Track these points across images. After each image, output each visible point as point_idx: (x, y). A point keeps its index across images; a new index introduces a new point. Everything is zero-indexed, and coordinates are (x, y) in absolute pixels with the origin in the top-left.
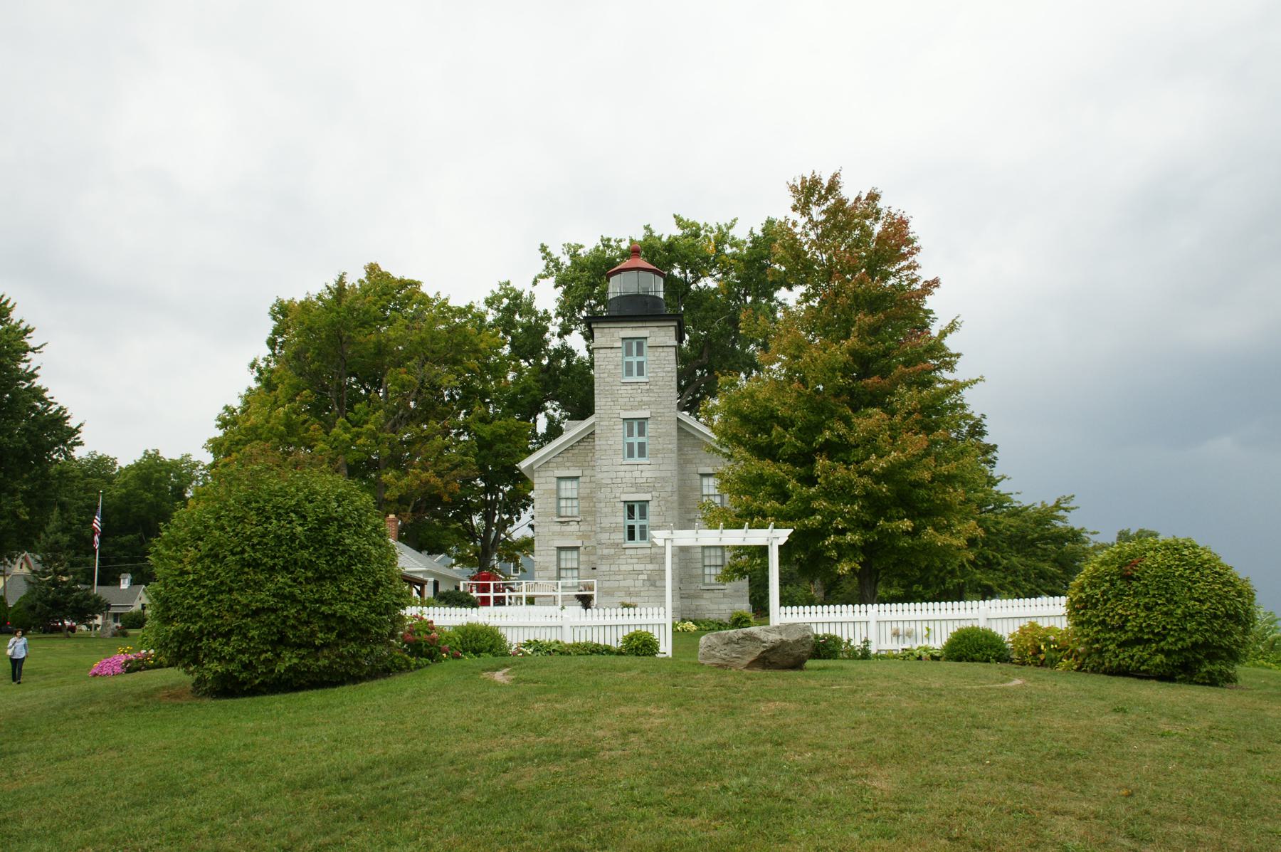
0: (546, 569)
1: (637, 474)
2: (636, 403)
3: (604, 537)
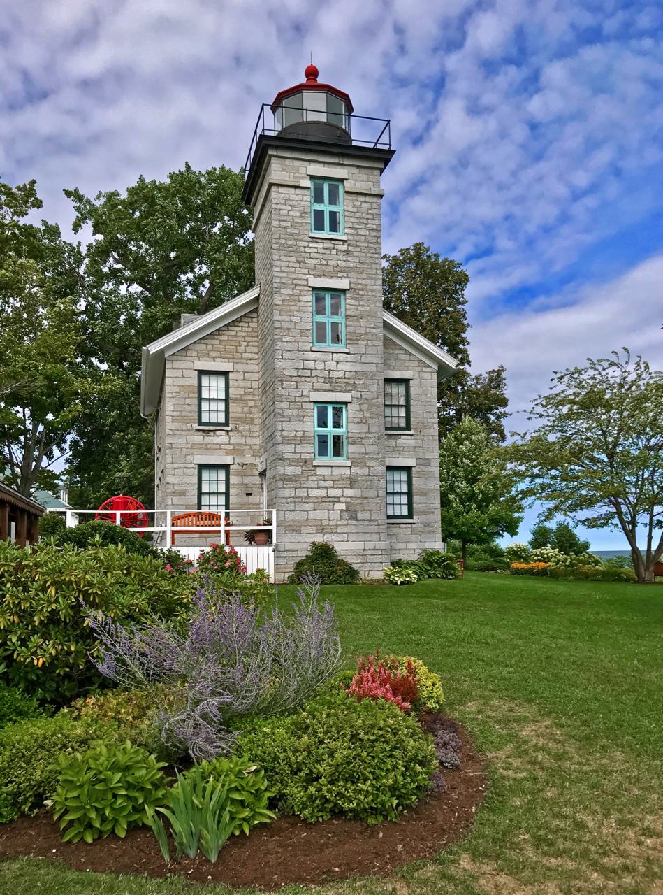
0: (182, 493)
1: (332, 365)
2: (330, 269)
3: (287, 450)
